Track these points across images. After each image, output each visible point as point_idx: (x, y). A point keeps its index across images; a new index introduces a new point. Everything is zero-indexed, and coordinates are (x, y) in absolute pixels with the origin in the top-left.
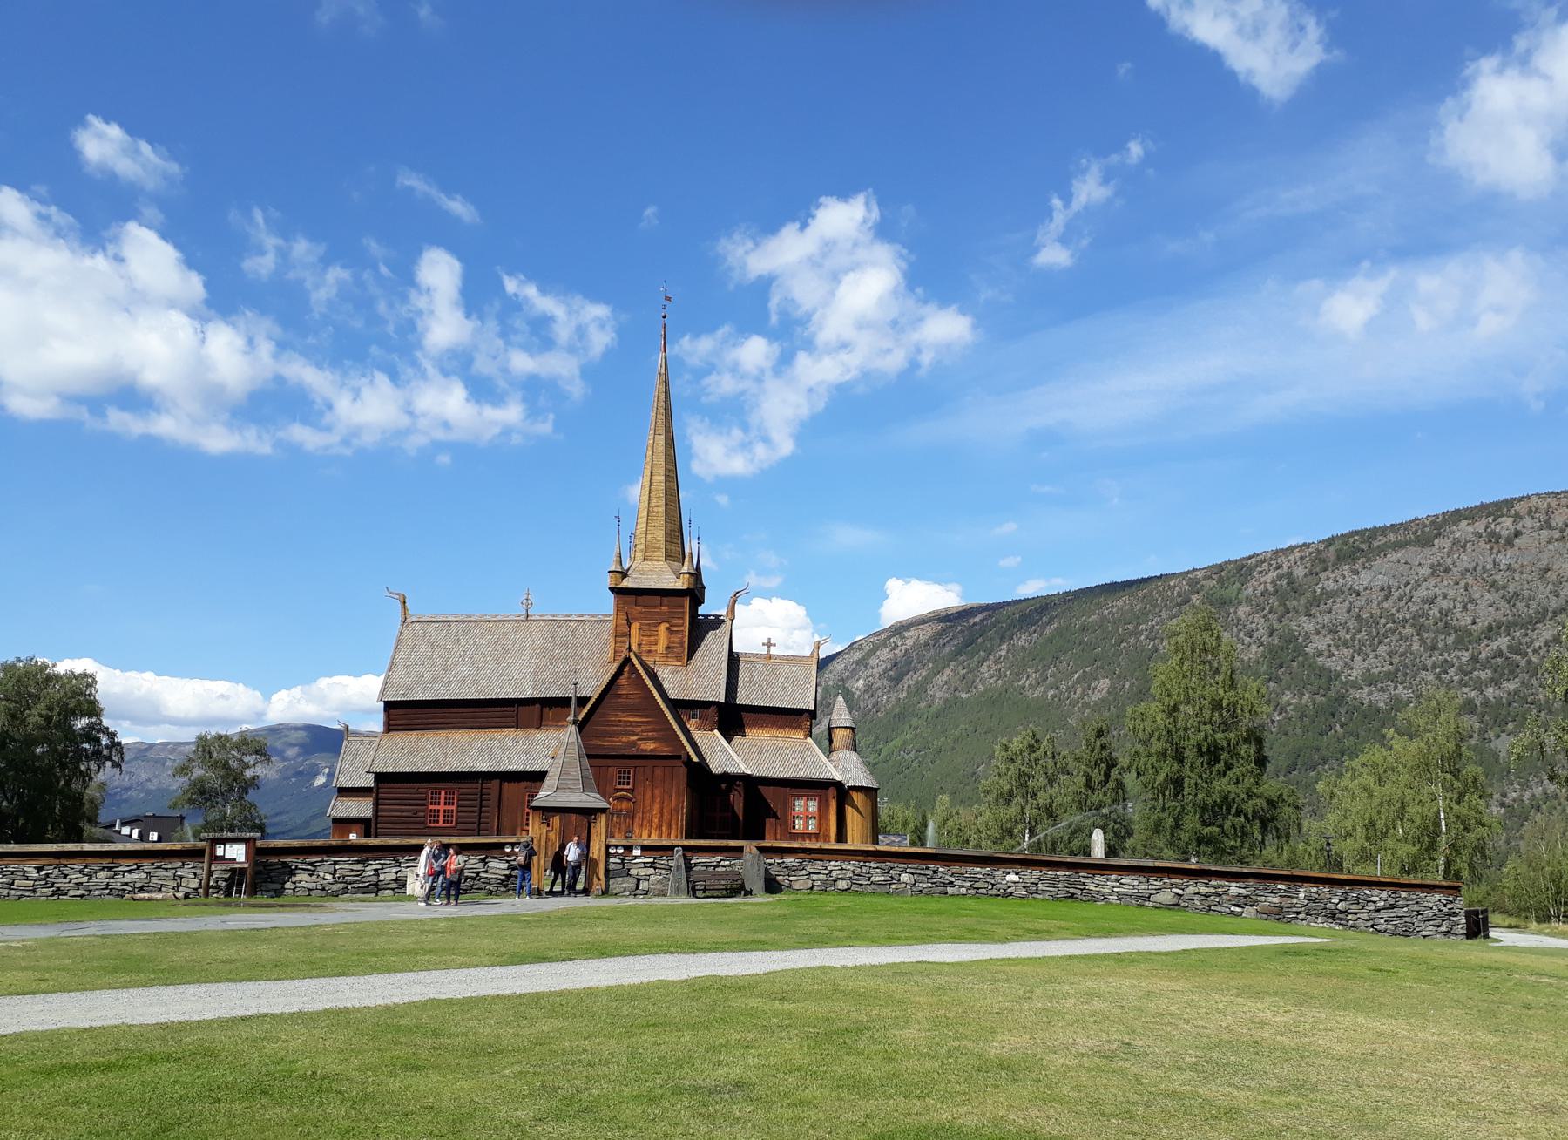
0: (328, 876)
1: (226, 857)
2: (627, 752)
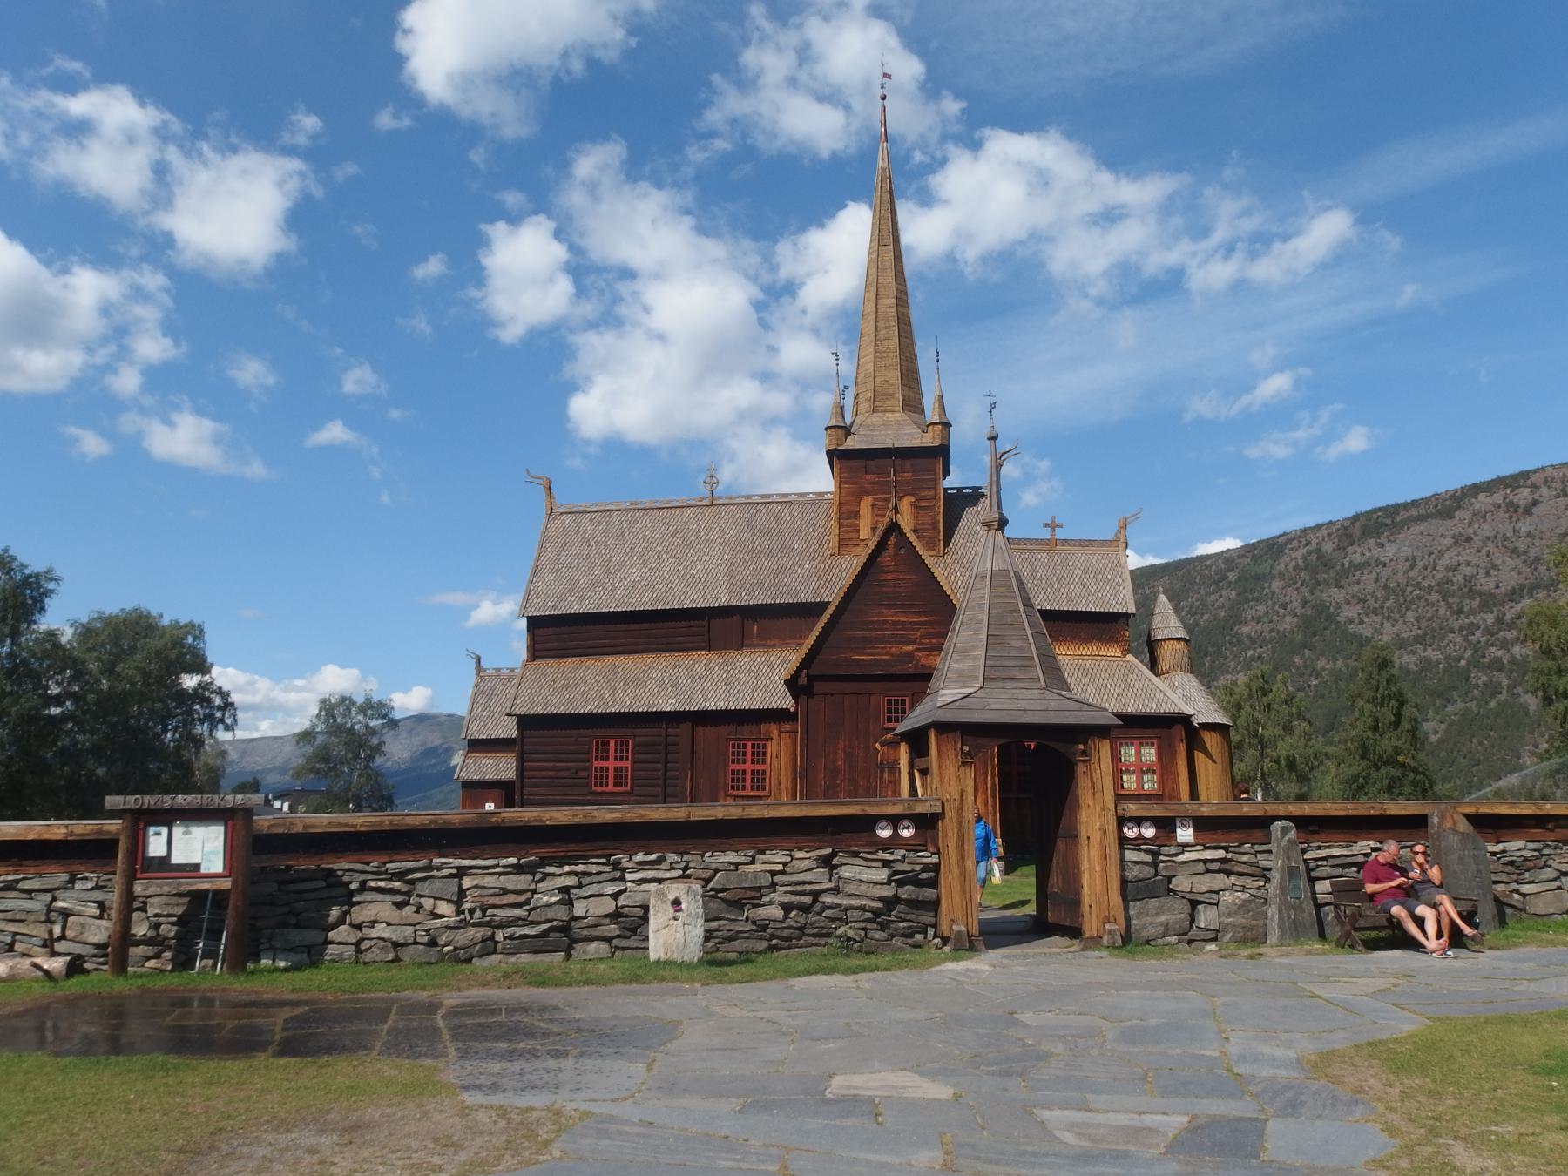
0: (445, 908)
1: (175, 860)
2: (898, 670)
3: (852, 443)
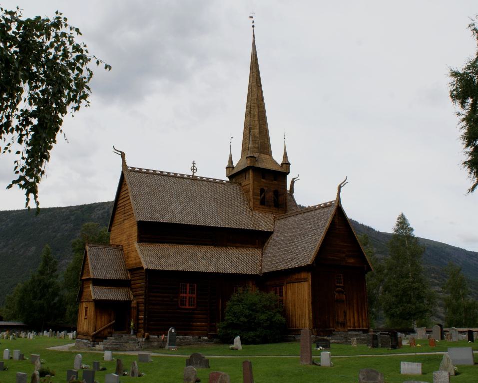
3: (257, 165)
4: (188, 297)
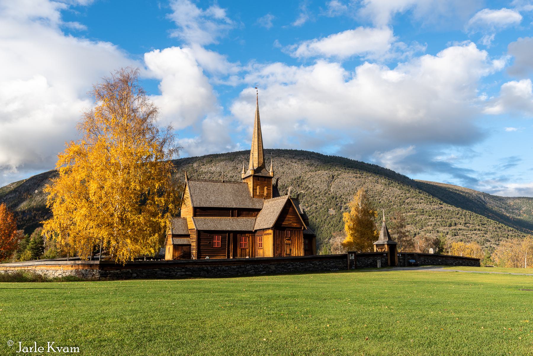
4: (217, 241)
